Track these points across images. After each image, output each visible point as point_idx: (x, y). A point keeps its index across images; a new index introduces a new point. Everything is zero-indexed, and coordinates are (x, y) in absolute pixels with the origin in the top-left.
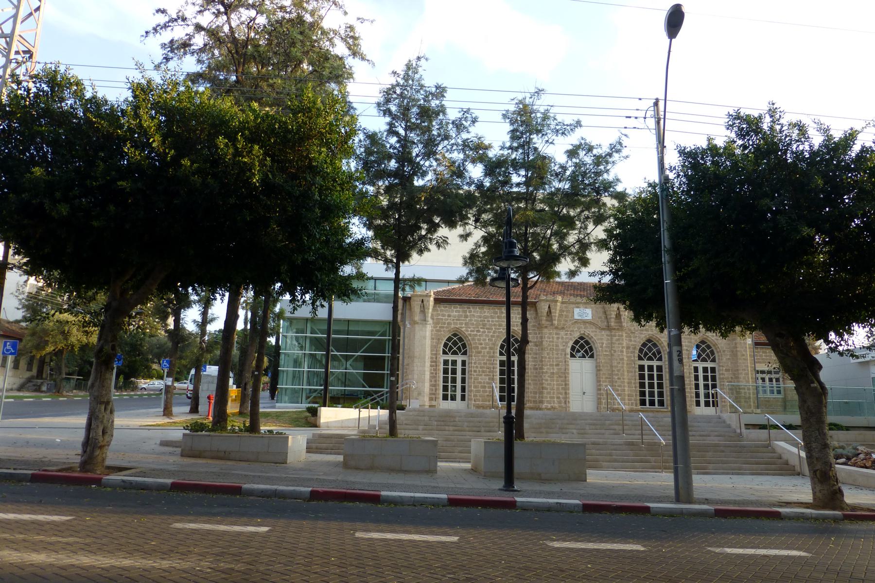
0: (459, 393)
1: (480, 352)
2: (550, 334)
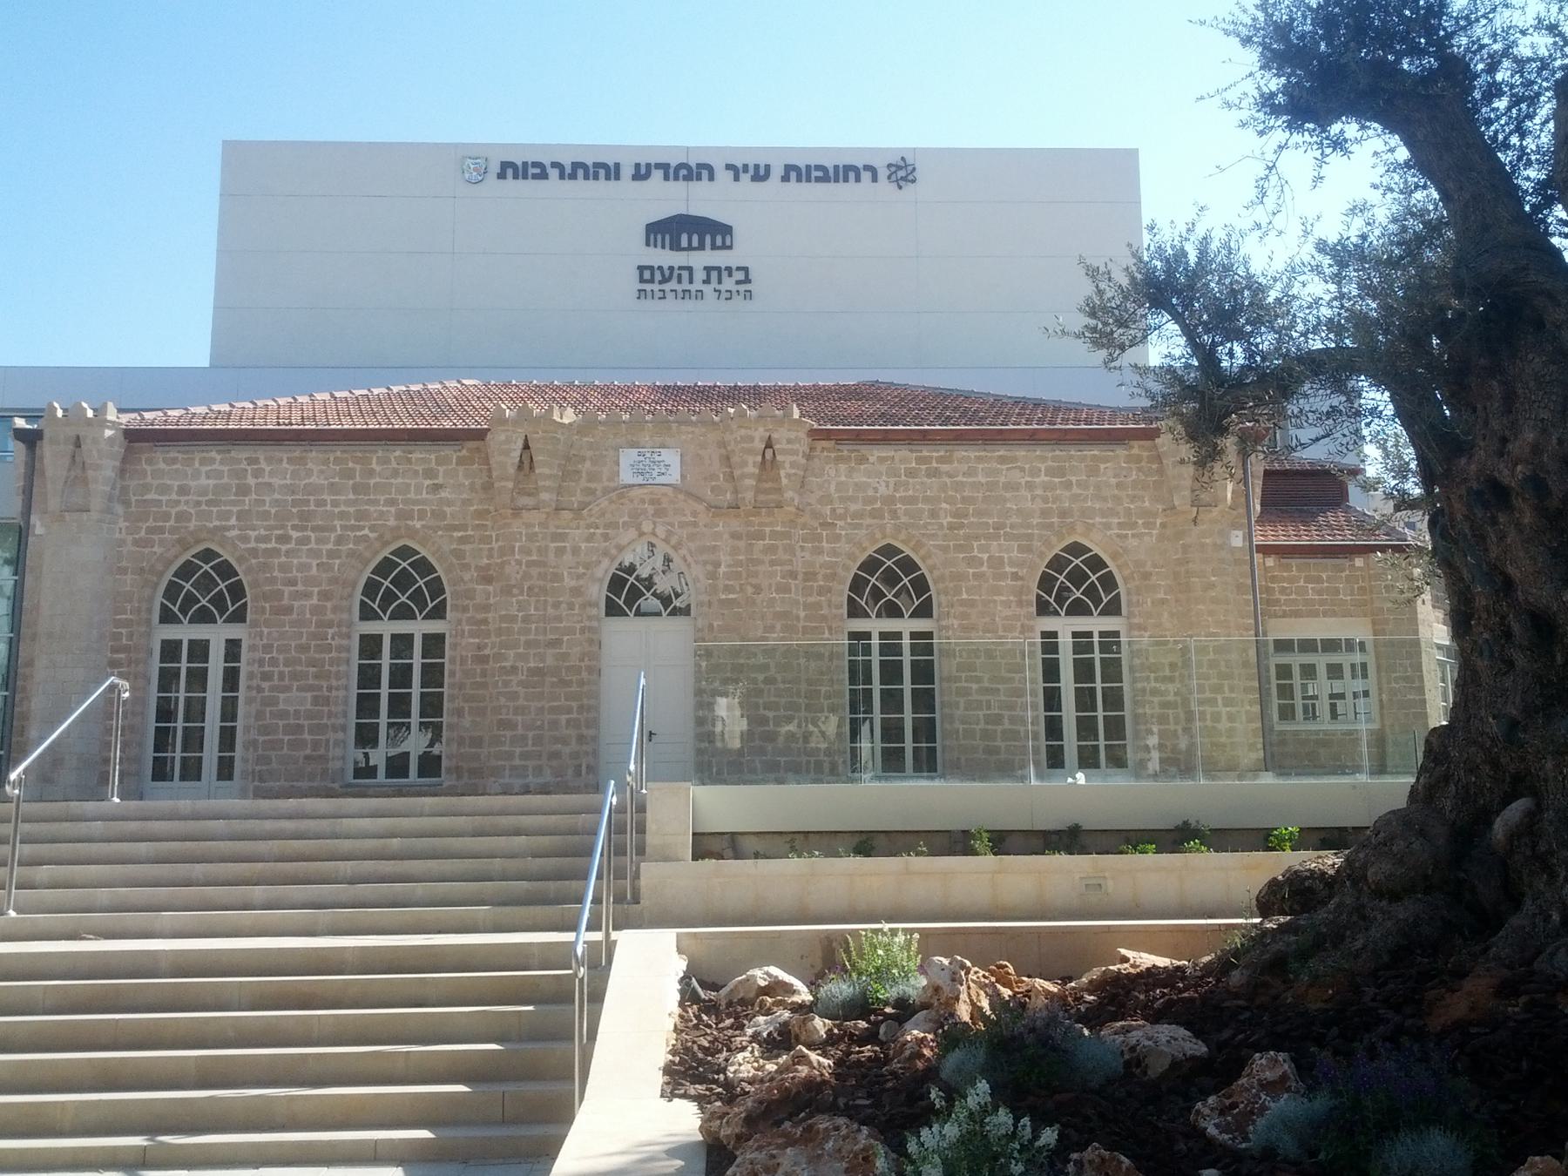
0: (210, 753)
1: (288, 610)
2: (532, 537)
